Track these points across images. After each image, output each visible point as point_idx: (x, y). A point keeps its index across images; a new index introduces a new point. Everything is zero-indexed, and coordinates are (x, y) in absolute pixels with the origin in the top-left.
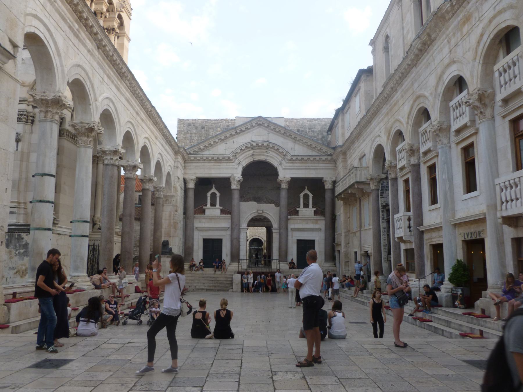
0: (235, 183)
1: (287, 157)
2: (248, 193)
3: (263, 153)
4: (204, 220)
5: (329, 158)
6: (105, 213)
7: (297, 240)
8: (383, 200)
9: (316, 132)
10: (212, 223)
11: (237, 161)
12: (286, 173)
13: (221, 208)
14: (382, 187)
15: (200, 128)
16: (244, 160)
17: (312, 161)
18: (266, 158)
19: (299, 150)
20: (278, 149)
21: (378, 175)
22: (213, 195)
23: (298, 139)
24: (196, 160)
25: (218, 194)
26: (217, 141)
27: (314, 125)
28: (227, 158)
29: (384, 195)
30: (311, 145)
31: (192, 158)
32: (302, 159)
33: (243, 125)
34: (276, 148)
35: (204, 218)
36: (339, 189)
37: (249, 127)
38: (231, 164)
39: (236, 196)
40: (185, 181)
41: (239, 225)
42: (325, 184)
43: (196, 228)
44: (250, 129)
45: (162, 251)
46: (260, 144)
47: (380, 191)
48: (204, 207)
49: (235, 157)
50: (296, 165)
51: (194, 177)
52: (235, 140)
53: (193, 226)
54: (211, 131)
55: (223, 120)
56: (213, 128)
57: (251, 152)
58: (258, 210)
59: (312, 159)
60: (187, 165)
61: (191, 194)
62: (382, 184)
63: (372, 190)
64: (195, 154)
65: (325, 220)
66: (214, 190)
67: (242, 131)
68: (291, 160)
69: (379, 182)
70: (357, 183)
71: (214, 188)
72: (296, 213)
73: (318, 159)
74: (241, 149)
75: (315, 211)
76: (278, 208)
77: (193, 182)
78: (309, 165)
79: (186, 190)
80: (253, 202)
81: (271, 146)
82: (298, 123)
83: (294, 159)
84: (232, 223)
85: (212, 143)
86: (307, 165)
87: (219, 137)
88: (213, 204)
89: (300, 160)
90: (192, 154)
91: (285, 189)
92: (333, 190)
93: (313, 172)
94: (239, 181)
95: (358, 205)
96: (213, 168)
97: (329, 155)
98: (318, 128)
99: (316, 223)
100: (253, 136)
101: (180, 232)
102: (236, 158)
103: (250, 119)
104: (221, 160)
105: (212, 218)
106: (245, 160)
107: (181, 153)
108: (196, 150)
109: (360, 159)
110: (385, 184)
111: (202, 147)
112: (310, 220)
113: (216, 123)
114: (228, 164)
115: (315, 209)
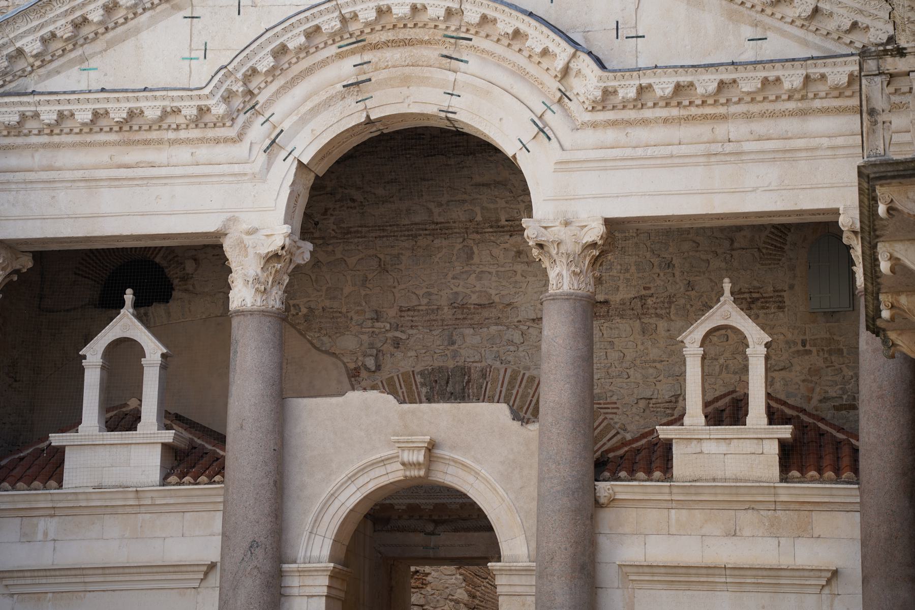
2: (397, 343)
4: (51, 525)
11: (258, 132)
13: (168, 436)
16: (303, 121)
18: (446, 102)
20: (517, 33)
25: (153, 350)
28: (189, 110)
35: (53, 512)
48: (56, 439)
50: (640, 134)
57: (346, 69)
65: (862, 508)
66: (125, 324)
72: (652, 458)
73: (792, 79)
74: (283, 50)
75: (783, 445)
76: (533, 427)
78: (736, 129)
80: (373, 395)
84: (225, 536)
85: (96, 16)
86: (721, 130)
88: (121, 418)
91: (568, 297)
93: (769, 174)
94: (275, 257)
99: (803, 531)
105: (123, 503)
106: (314, 119)
111: (32, 46)
112: (752, 506)
114: (204, 152)
115: (786, 431)
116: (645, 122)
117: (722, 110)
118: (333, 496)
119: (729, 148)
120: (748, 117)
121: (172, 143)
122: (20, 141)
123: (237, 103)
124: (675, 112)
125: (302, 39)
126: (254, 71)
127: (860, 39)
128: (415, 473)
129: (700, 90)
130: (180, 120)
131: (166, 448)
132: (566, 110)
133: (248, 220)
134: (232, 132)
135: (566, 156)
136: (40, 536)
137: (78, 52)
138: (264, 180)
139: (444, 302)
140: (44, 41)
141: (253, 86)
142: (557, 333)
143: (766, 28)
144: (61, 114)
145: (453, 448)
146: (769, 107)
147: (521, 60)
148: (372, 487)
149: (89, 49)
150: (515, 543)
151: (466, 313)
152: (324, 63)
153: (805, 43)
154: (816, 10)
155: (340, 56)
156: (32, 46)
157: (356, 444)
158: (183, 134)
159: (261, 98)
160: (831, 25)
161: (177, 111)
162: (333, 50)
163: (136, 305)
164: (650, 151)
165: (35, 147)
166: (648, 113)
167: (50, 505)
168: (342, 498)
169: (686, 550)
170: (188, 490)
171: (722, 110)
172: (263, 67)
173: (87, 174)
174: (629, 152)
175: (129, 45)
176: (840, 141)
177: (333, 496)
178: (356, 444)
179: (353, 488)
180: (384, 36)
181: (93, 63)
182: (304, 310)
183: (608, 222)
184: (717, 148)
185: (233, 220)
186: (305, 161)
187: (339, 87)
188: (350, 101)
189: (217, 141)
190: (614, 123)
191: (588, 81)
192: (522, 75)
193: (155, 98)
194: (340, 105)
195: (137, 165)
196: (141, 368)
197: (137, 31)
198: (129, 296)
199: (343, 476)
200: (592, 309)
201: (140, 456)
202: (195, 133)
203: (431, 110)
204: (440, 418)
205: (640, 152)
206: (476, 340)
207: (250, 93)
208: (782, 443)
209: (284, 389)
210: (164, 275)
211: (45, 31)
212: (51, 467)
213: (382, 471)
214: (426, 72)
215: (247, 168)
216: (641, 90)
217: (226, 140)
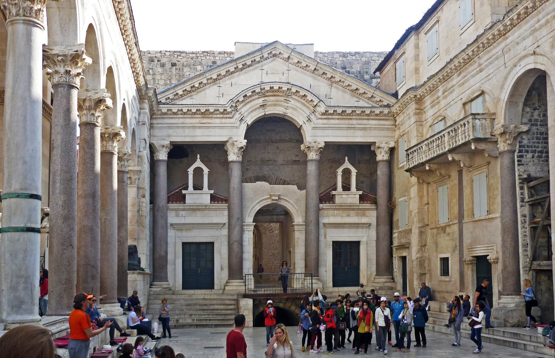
0: (236, 151)
1: (318, 109)
3: (281, 103)
4: (183, 213)
5: (386, 111)
6: (58, 185)
7: (334, 242)
8: (522, 168)
9: (353, 73)
11: (237, 116)
12: (317, 135)
14: (520, 146)
15: (168, 66)
16: (249, 114)
17: (358, 115)
18: (285, 111)
19: (341, 98)
20: (305, 96)
21: (516, 127)
22: (198, 172)
23: (337, 79)
24: (171, 114)
25: (206, 170)
26: (205, 81)
27: (350, 63)
29: (524, 160)
30: (357, 89)
31: (164, 110)
32: (343, 111)
33: (248, 55)
34: (302, 93)
35: (184, 210)
36: (402, 162)
37: (258, 59)
38: (228, 120)
40: (152, 149)
42: (378, 152)
43: (171, 225)
44: (259, 62)
45: (129, 264)
46: (276, 88)
47: (516, 154)
48: (184, 192)
49: (236, 109)
50: (332, 121)
51: (167, 143)
52: (233, 80)
53: (166, 223)
54: (185, 69)
55: (206, 53)
56: (189, 66)
57: (260, 101)
59: (358, 112)
60: (155, 121)
61: (162, 171)
62: (520, 142)
63: (500, 153)
64: (168, 104)
66: (198, 163)
67: (245, 66)
68: (326, 113)
69: (515, 138)
70: (477, 140)
71: (198, 160)
73: (368, 111)
74: (245, 96)
77: (164, 149)
78: (354, 122)
79: (153, 163)
81: (294, 90)
82: (326, 59)
83: (331, 111)
85: (197, 85)
86: (351, 122)
87: (208, 75)
89: (339, 114)
90: (164, 104)
92: (390, 163)
93: (360, 133)
95: (456, 182)
97: (385, 106)
98: (356, 68)
100: (263, 75)
101: (147, 232)
102: (237, 111)
103: (258, 47)
107: (149, 99)
108: (171, 96)
109: (464, 104)
110: (525, 142)
111: (180, 92)
113: (196, 57)
116: (333, 119)
117: (351, 117)
119: (353, 126)
120: (356, 119)
121: (214, 118)
122: (176, 116)
123: (233, 109)
124: (340, 117)
125: (251, 93)
126: (238, 101)
127: (381, 104)
129: (347, 112)
130: (218, 112)
131: (211, 194)
132: (315, 115)
133: (235, 139)
134: (231, 116)
135: (315, 126)
137: (191, 94)
138: (238, 128)
139: (259, 159)
140: (183, 91)
141: (237, 104)
142: (312, 168)
143: (360, 99)
144: (188, 110)
145: (284, 196)
146: (361, 117)
147: (304, 102)
149: (193, 93)
150: (298, 219)
151: (264, 162)
152: (255, 99)
153: (368, 103)
154: (372, 96)
155: (258, 98)
156: (180, 92)
157: (258, 195)
158: (218, 116)
159: (239, 108)
160: (375, 100)
161: (218, 110)
162: (257, 96)
163: (200, 158)
164: (335, 126)
165: (179, 118)
166: (334, 117)
169: (338, 220)
170: (216, 205)
171: (351, 117)
172: (240, 100)
173: (193, 125)
174: (330, 126)
175: (203, 92)
176: (376, 126)
178: (258, 195)
180: (270, 94)
181: (193, 97)
183: (325, 142)
184: (350, 126)
185: (231, 138)
186: (249, 124)
187: (259, 106)
188: (261, 109)
189: (227, 118)
190: (326, 119)
191: (322, 108)
192: (304, 105)
194: (258, 111)
195: (206, 123)
197: (205, 89)
198: (198, 156)
200: (320, 162)
201: (204, 196)
202: (221, 116)
203: (281, 113)
204: (280, 189)
205: (332, 126)
206: (268, 169)
207: (236, 106)
208: (360, 195)
209: (245, 180)
210: (215, 151)
211: (184, 89)
212: (182, 199)
214: (281, 103)
215: (235, 125)
216: (334, 111)
217: (231, 118)
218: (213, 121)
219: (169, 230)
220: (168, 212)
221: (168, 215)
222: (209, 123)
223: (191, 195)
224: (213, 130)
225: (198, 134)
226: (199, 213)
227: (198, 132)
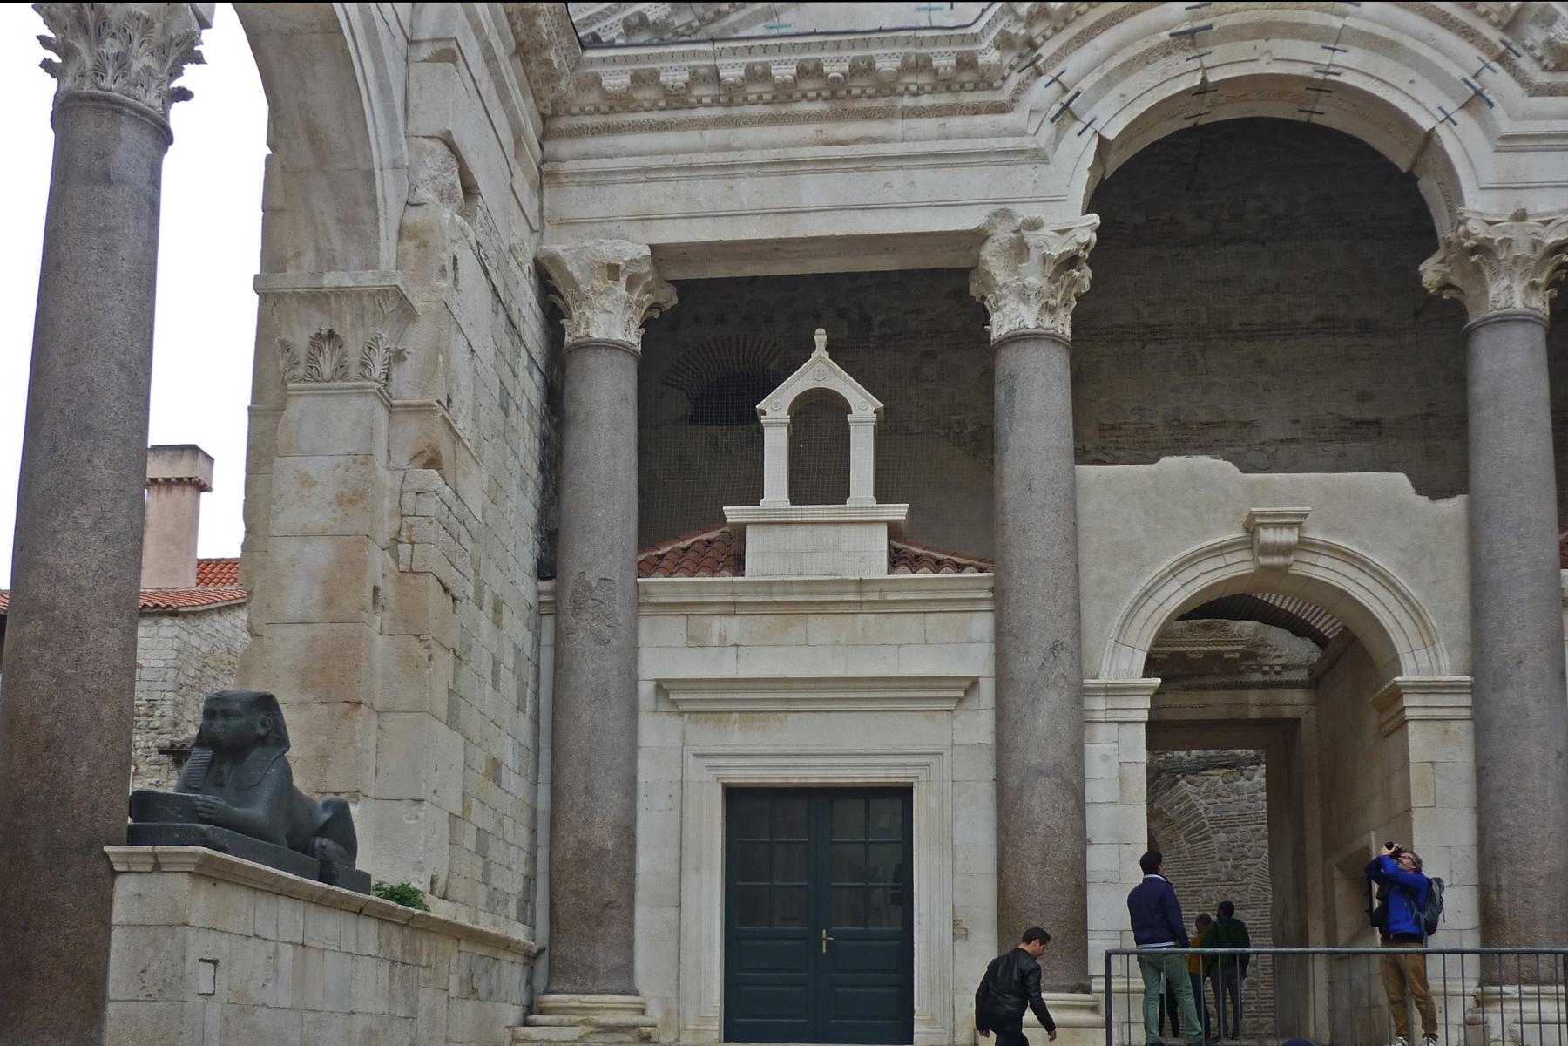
4: (732, 627)
10: (819, 641)
28: (944, 61)
35: (733, 609)
39: (1038, 404)
41: (1072, 647)
58: (1251, 527)
71: (820, 353)
96: (823, 165)
104: (887, 87)
118: (1147, 593)
121: (907, 113)
128: (1278, 560)
130: (924, 79)
131: (894, 530)
136: (715, 640)
148: (1202, 583)
158: (925, 100)
163: (827, 349)
167: (730, 599)
168: (1159, 597)
177: (1147, 593)
179: (1175, 584)
182: (971, 428)
193: (895, 41)
195: (857, 141)
196: (848, 427)
199: (1163, 566)
201: (852, 539)
202: (943, 99)
213: (1219, 562)
218: (898, 127)
219: (646, 722)
220: (645, 625)
221: (644, 637)
222: (874, 140)
223: (778, 530)
224: (897, 177)
225: (808, 201)
226: (820, 627)
227: (813, 189)
